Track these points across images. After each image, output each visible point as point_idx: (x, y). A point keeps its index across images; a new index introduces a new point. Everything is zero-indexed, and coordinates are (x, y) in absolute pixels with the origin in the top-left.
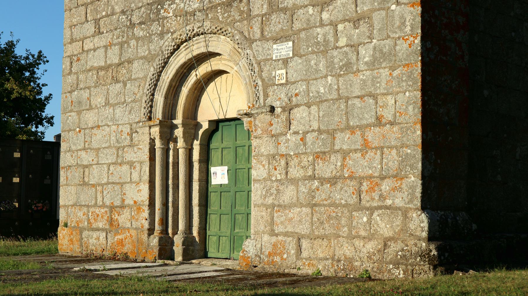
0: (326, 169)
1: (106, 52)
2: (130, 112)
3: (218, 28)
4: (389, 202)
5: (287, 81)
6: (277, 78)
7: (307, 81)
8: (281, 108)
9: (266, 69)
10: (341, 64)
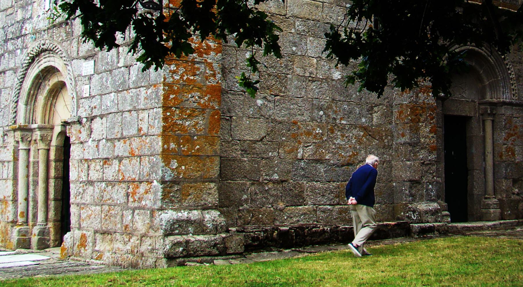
0: (111, 172)
3: (54, 46)
4: (143, 203)
5: (90, 95)
7: (101, 95)
8: (86, 118)
9: (79, 83)
10: (120, 82)
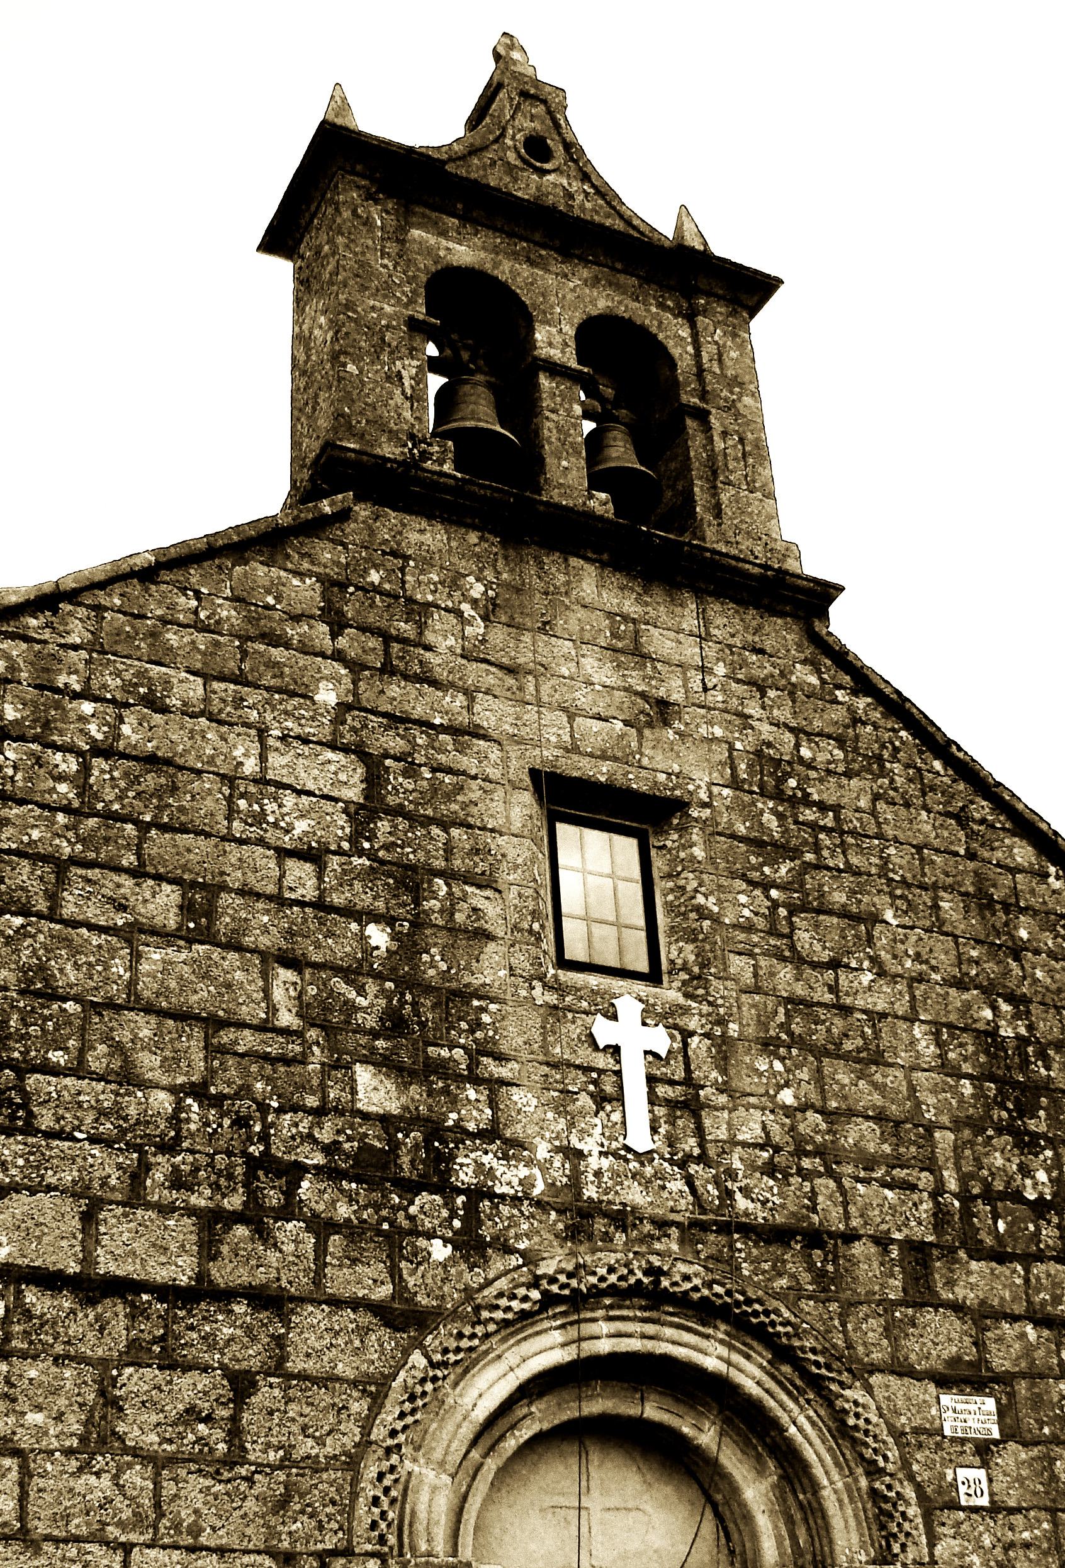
1: (89, 1219)
2: (283, 1504)
5: (992, 1502)
6: (962, 1489)
